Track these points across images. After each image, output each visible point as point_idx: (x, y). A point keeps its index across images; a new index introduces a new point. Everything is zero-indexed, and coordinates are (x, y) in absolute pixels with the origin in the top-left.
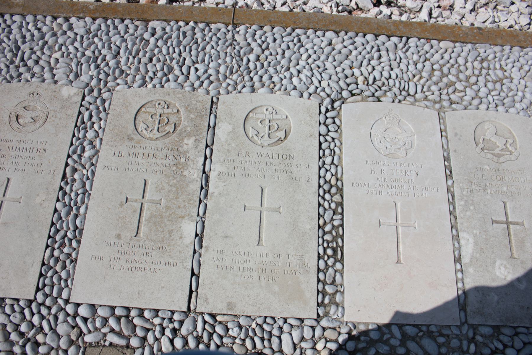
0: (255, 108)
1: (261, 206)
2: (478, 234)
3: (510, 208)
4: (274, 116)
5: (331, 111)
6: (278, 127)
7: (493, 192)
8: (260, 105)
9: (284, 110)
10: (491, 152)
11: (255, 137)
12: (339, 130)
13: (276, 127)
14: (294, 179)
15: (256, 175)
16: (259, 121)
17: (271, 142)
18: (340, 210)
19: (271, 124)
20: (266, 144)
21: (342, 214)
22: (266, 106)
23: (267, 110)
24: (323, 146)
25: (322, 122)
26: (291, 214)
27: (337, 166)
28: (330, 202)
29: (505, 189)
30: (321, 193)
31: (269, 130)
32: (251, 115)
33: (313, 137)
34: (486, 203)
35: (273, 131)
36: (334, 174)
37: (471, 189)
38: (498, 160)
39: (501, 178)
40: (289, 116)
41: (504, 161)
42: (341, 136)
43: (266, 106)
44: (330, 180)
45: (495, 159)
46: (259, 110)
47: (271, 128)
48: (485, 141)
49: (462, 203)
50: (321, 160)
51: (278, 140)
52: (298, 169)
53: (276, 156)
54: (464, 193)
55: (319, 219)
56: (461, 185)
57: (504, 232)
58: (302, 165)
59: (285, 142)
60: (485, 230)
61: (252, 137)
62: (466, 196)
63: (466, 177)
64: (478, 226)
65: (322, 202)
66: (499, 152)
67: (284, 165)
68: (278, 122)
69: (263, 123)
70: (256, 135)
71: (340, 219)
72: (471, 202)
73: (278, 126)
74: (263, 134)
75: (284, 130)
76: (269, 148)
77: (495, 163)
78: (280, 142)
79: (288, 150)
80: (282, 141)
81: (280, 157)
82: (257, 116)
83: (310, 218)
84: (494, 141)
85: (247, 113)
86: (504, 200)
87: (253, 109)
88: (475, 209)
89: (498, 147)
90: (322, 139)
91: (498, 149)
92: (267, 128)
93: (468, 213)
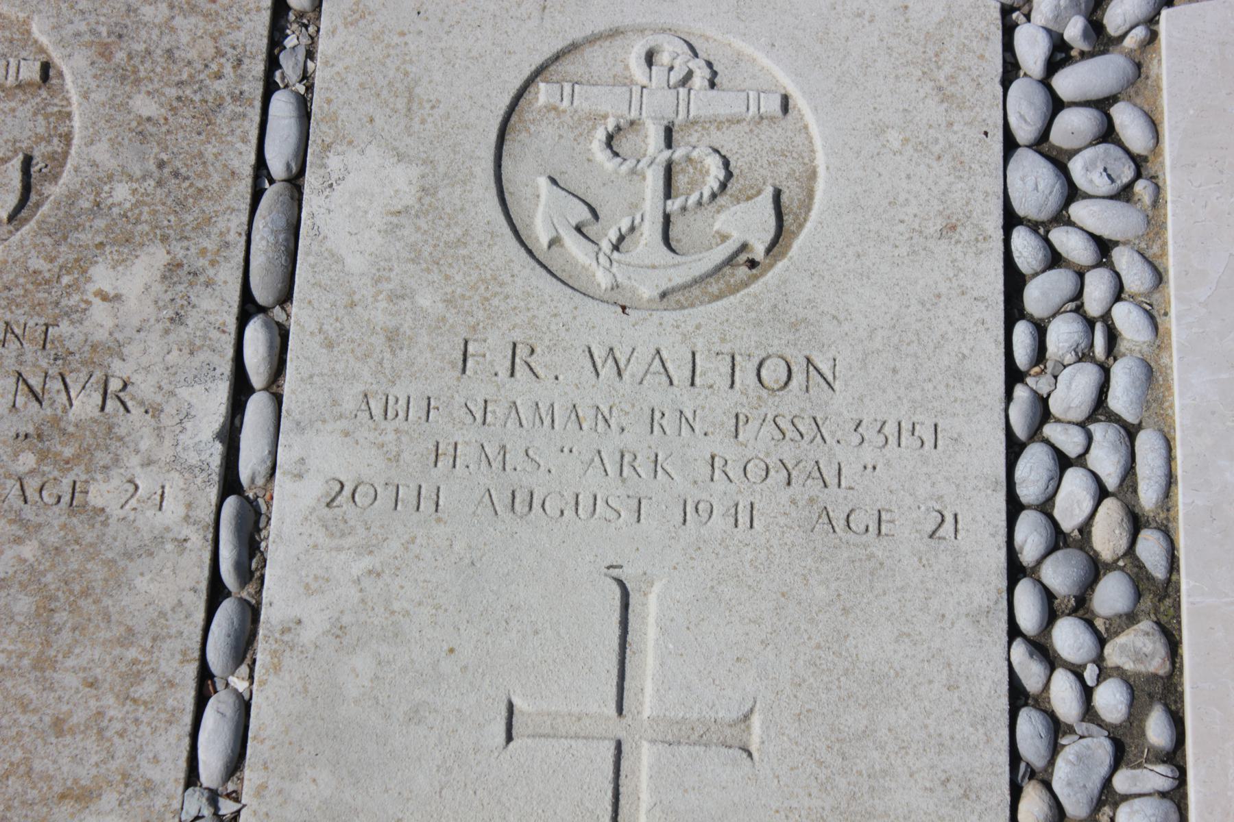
0: (573, 48)
1: (620, 709)
4: (701, 101)
5: (1084, 55)
6: (729, 175)
8: (602, 25)
9: (764, 60)
11: (572, 242)
12: (1141, 187)
13: (715, 172)
14: (840, 524)
15: (586, 502)
16: (601, 135)
17: (680, 276)
18: (1157, 730)
19: (679, 153)
20: (647, 292)
21: (1174, 756)
22: (641, 31)
23: (650, 59)
24: (1036, 297)
25: (1024, 132)
26: (820, 763)
27: (1131, 432)
28: (1090, 674)
30: (1029, 615)
31: (668, 195)
32: (543, 93)
33: (966, 234)
35: (694, 198)
36: (1111, 483)
40: (799, 100)
42: (1154, 224)
43: (641, 31)
44: (1085, 528)
46: (596, 57)
47: (680, 181)
50: (1020, 392)
51: (730, 261)
52: (868, 455)
53: (713, 370)
55: (1016, 792)
58: (890, 429)
59: (771, 277)
61: (554, 242)
65: (1031, 673)
67: (769, 429)
68: (728, 141)
69: (623, 145)
70: (578, 229)
71: (1163, 795)
73: (726, 163)
74: (625, 225)
75: (769, 192)
76: (670, 317)
78: (743, 271)
79: (794, 327)
80: (752, 264)
81: (745, 375)
82: (588, 99)
83: (956, 791)
85: (517, 83)
87: (557, 58)
90: (1025, 246)
92: (653, 181)
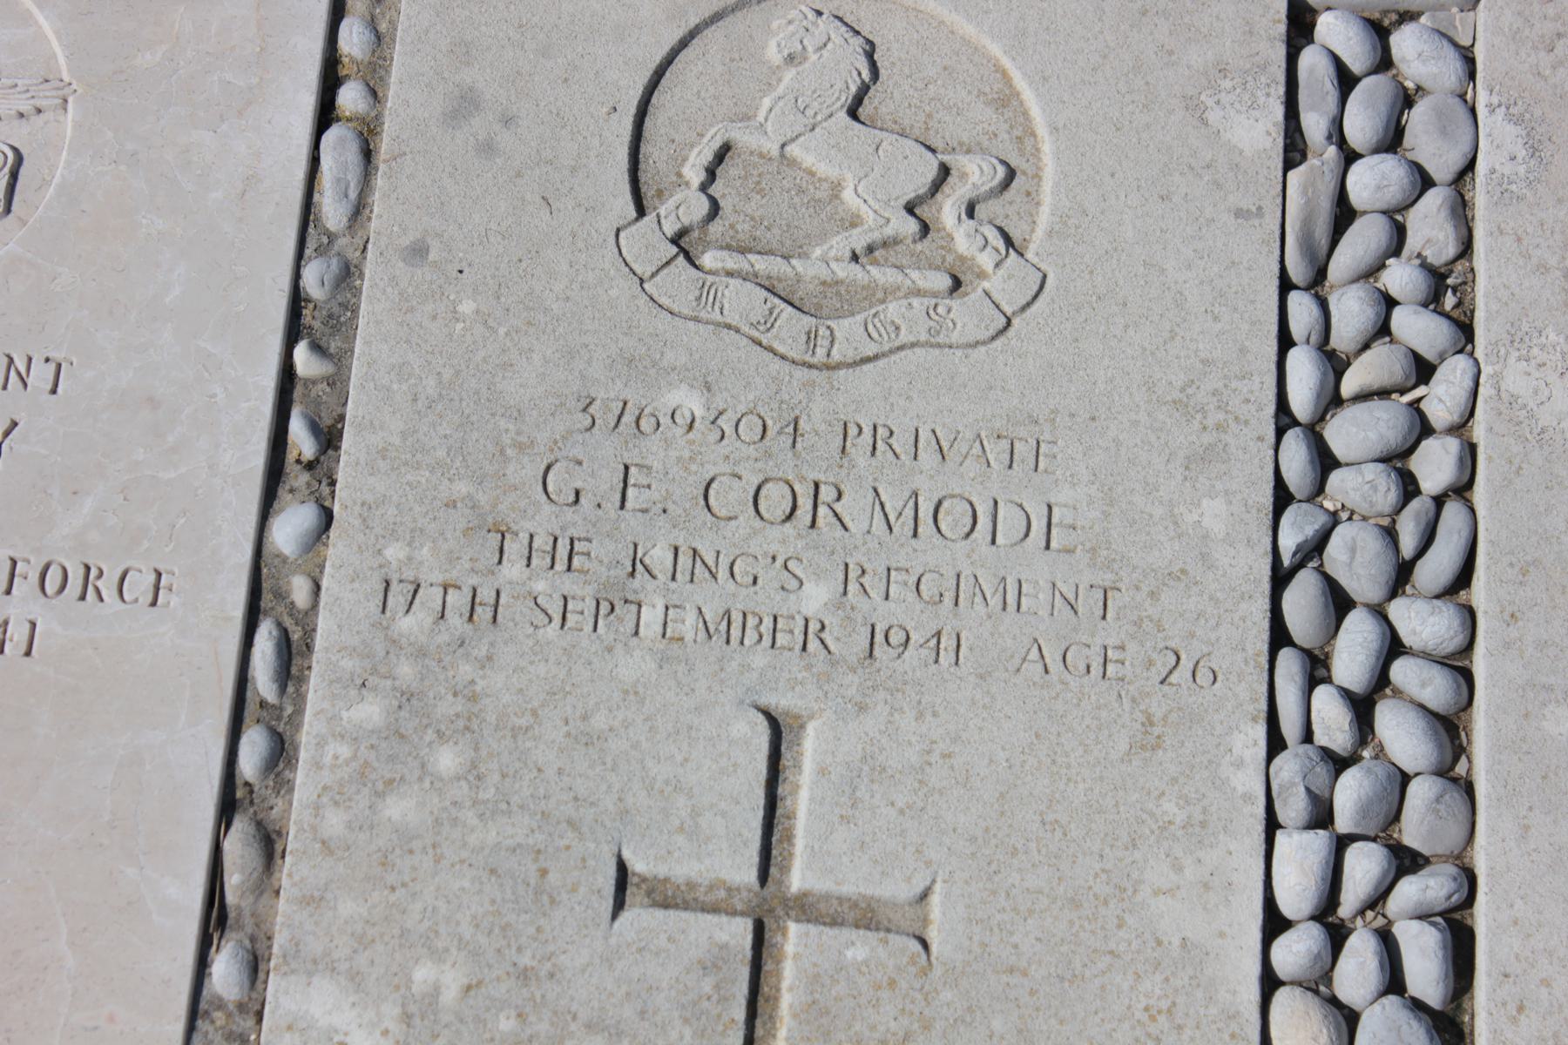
2: (450, 995)
3: (822, 771)
7: (688, 625)
10: (761, 264)
29: (815, 598)
34: (600, 721)
37: (486, 595)
38: (811, 337)
39: (805, 503)
41: (870, 349)
45: (790, 328)
48: (728, 171)
49: (370, 712)
54: (411, 625)
56: (394, 553)
57: (707, 986)
60: (526, 960)
62: (421, 653)
63: (462, 488)
64: (467, 931)
66: (844, 270)
72: (448, 707)
77: (776, 365)
84: (823, 169)
86: (780, 701)
88: (473, 773)
89: (854, 222)
91: (840, 244)
93: (398, 809)
